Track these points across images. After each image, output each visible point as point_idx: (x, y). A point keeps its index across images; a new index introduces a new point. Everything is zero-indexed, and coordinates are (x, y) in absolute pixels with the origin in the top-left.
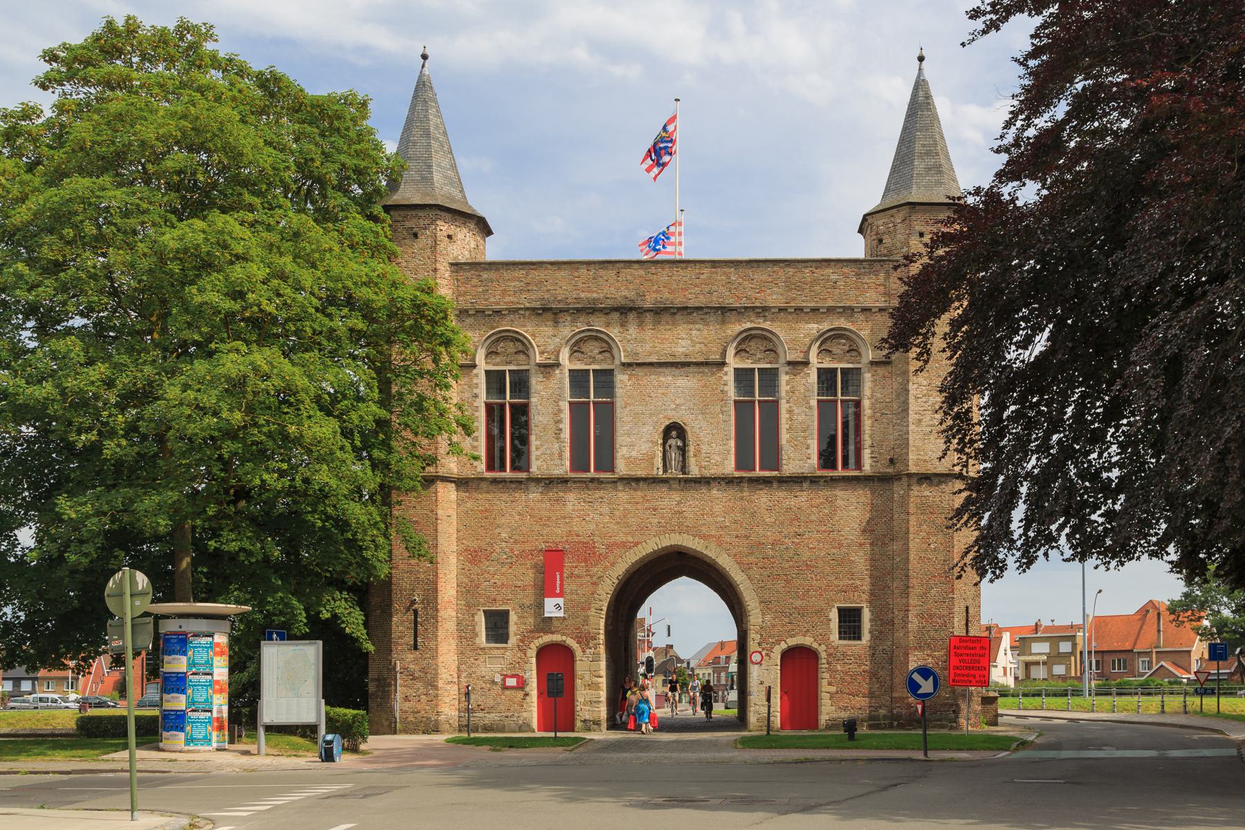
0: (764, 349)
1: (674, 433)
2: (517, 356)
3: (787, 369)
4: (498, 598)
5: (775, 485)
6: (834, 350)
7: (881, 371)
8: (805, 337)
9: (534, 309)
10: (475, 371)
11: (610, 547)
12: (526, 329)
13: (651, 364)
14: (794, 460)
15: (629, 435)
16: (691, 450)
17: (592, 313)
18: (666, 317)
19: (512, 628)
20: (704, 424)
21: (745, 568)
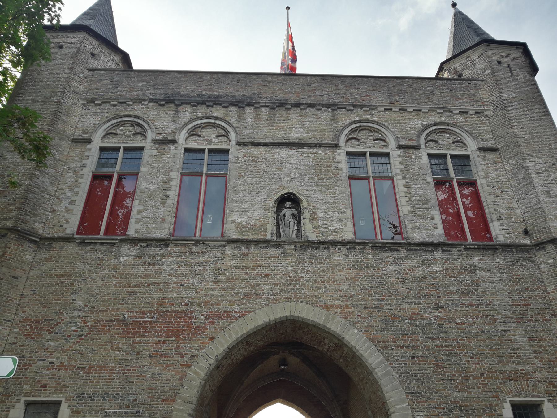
0: (373, 138)
2: (134, 137)
3: (399, 152)
4: (53, 383)
5: (403, 253)
7: (490, 156)
8: (412, 129)
10: (89, 146)
11: (210, 318)
13: (266, 145)
14: (419, 229)
15: (241, 202)
17: (212, 106)
18: (281, 113)
20: (319, 195)
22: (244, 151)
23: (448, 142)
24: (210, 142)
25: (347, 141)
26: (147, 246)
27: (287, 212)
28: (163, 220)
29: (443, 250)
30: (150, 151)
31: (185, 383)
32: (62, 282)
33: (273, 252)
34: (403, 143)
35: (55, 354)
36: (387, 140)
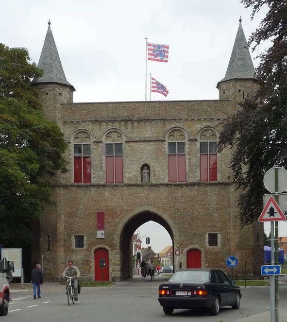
1: (146, 167)
3: (188, 142)
6: (207, 135)
9: (92, 121)
11: (122, 211)
12: (88, 127)
13: (137, 141)
16: (152, 174)
18: (142, 123)
19: (85, 243)
21: (174, 219)
27: (145, 171)
28: (102, 177)
29: (198, 186)
30: (93, 147)
33: (141, 188)
34: (191, 138)
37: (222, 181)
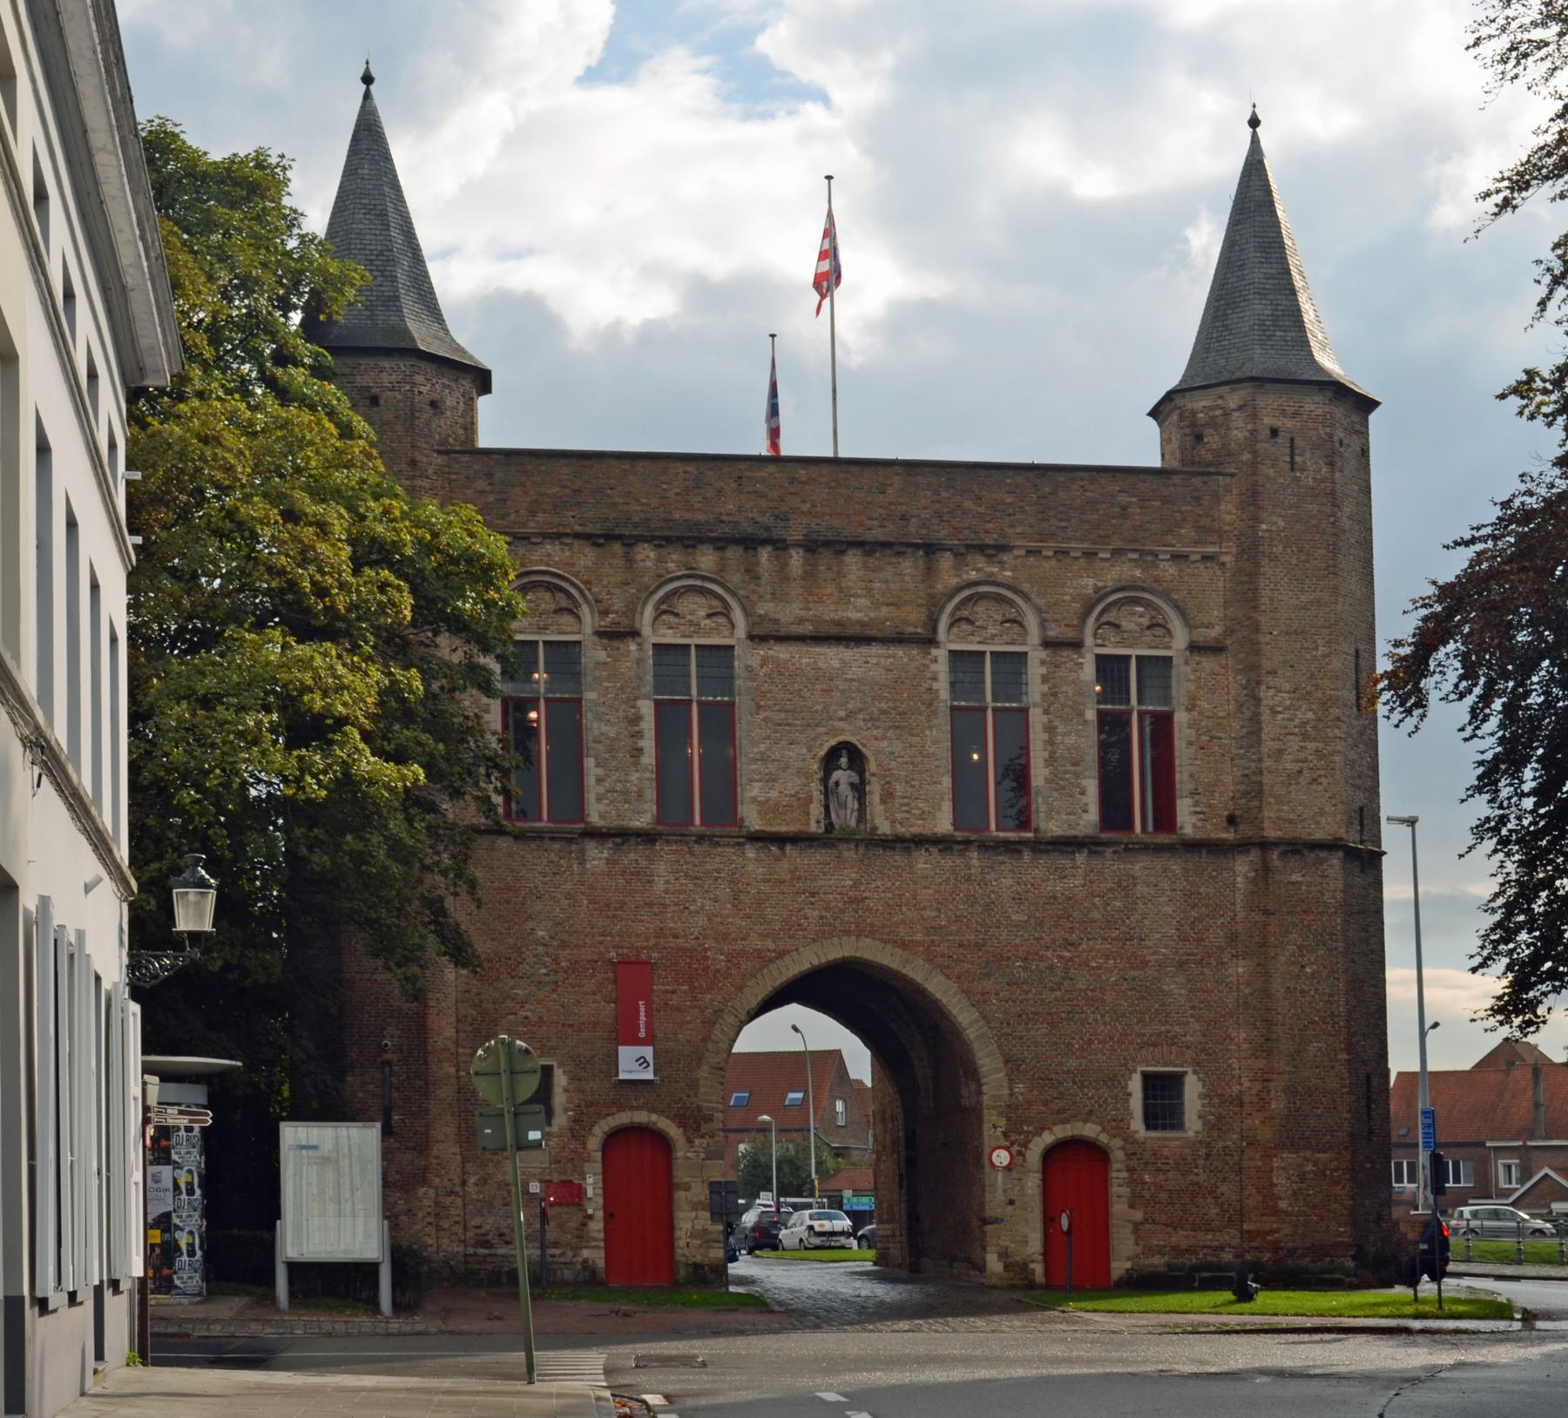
0: (1000, 618)
3: (1043, 654)
5: (1027, 856)
20: (897, 747)
22: (762, 652)
23: (1140, 625)
24: (696, 628)
25: (951, 625)
26: (623, 844)
27: (843, 776)
29: (1091, 852)
31: (710, 1046)
32: (508, 902)
34: (1052, 633)
35: (527, 1006)
36: (1026, 623)
37: (1200, 835)
